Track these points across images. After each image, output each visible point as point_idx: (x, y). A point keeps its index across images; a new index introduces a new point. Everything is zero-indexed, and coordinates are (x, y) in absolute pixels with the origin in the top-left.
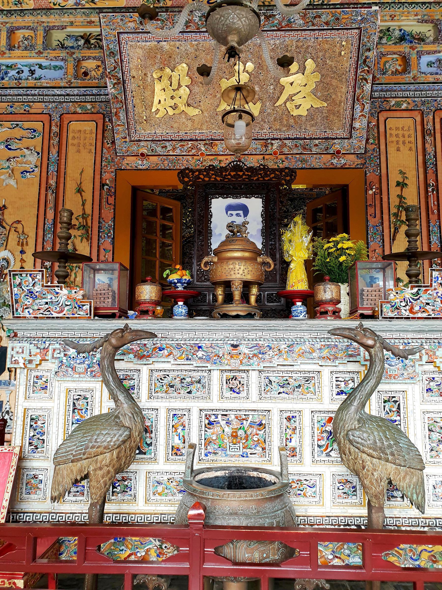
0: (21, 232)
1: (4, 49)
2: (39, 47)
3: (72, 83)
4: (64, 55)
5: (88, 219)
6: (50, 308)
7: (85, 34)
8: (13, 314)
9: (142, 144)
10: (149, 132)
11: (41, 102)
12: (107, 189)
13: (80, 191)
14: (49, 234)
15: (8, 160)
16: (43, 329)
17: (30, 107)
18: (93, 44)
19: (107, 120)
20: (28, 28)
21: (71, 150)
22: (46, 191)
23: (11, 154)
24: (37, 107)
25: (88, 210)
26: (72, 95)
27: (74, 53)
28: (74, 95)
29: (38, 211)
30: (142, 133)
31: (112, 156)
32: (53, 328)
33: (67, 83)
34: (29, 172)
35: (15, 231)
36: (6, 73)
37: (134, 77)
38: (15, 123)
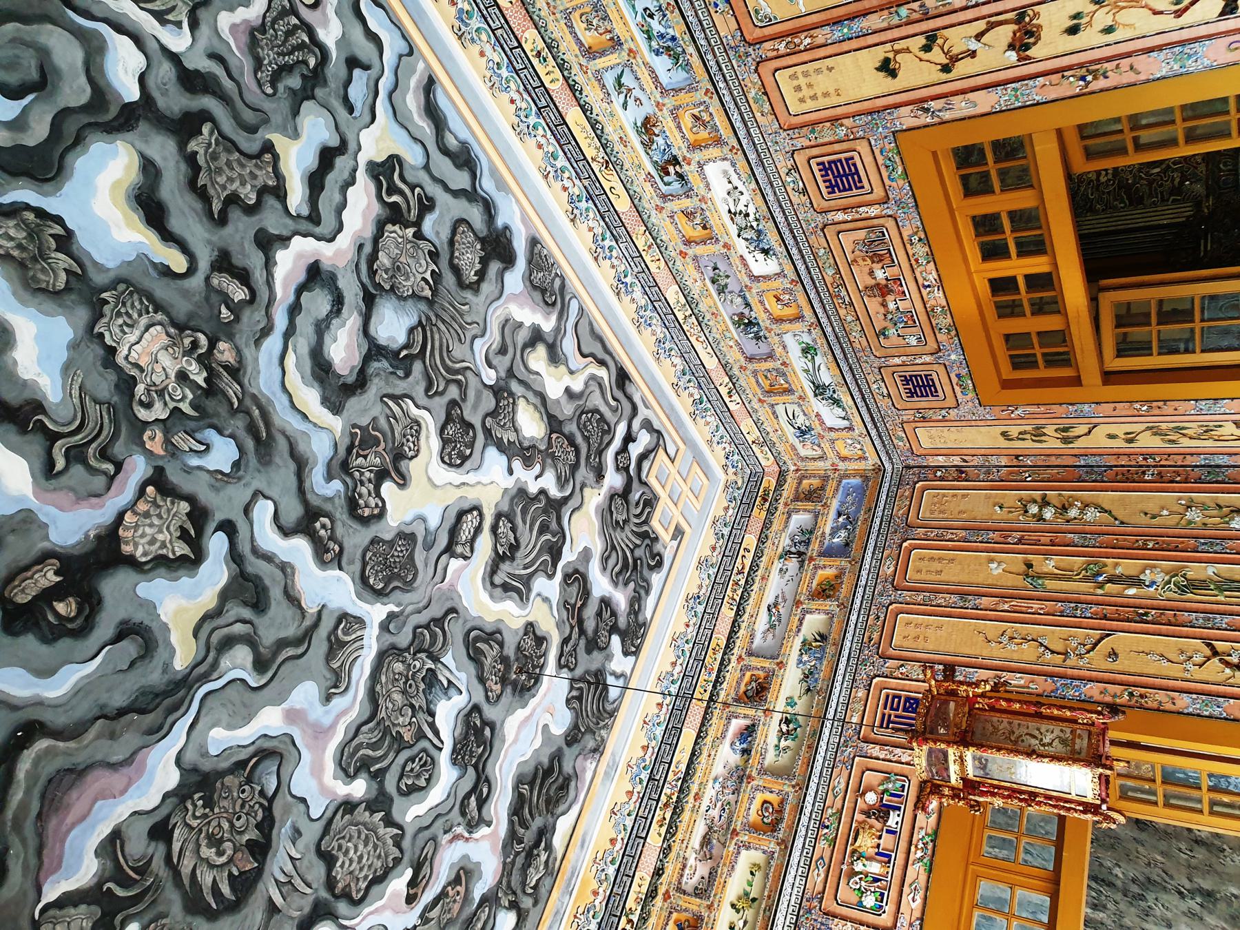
1: (625, 54)
36: (662, 36)
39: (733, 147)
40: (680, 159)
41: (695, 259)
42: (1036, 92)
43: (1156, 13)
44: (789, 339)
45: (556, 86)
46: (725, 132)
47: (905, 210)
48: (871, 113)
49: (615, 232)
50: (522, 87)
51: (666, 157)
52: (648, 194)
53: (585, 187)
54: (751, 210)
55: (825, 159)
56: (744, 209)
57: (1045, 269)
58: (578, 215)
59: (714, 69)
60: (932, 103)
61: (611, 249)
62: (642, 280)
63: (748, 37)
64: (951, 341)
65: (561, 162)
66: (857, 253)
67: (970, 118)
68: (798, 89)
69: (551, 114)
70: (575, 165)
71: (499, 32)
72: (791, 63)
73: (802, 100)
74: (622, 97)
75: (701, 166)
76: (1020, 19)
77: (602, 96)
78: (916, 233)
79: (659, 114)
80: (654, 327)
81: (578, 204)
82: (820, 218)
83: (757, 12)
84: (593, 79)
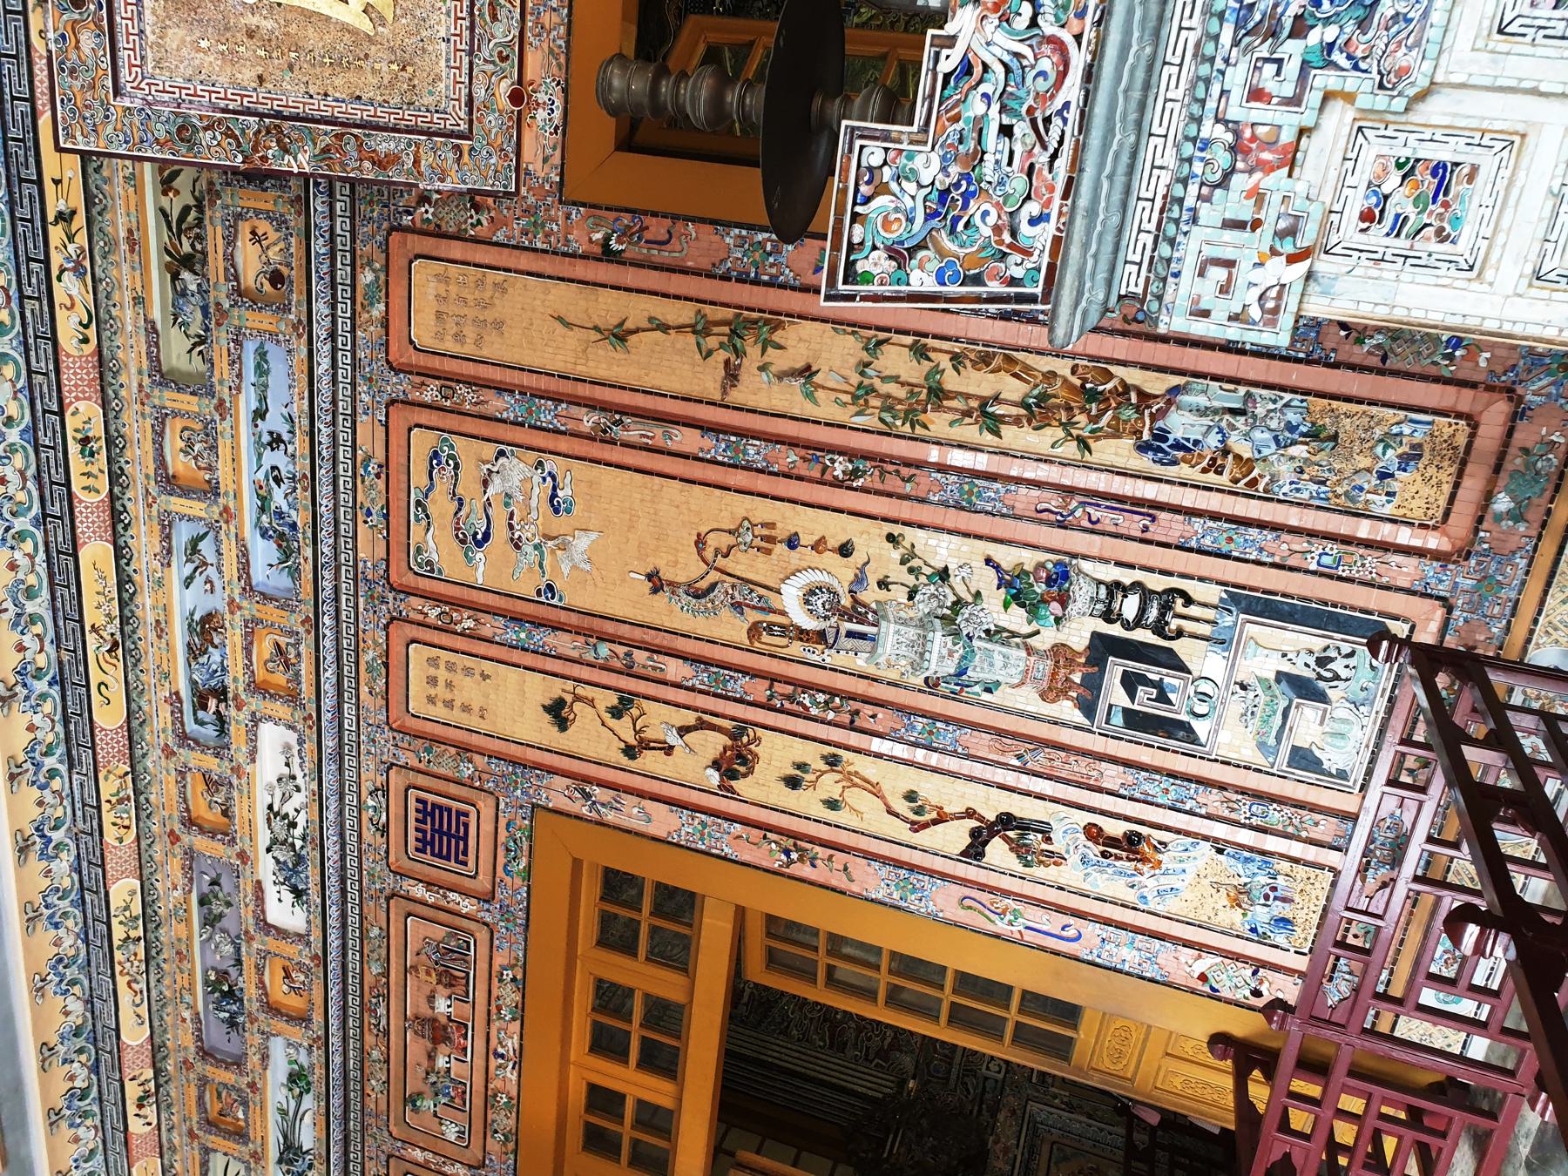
0: (731, 540)
1: (216, 510)
2: (207, 406)
3: (300, 321)
4: (224, 334)
5: (710, 318)
6: (1030, 110)
7: (168, 266)
8: (1032, 299)
9: (480, 93)
10: (443, 63)
11: (354, 423)
12: (619, 241)
13: (620, 335)
14: (745, 453)
15: (518, 547)
16: (1134, 155)
17: (368, 459)
18: (193, 246)
19: (406, 220)
20: (159, 435)
21: (493, 349)
22: (613, 442)
23: (500, 533)
24: (369, 437)
25: (682, 313)
26: (334, 323)
27: (218, 304)
28: (334, 316)
29: (674, 478)
30: (447, 87)
31: (518, 213)
32: (1136, 94)
33: (300, 336)
34: (554, 488)
35: (726, 556)
36: (280, 514)
37: (261, 79)
38: (412, 509)
39: (310, 716)
40: (230, 695)
41: (190, 854)
42: (729, 841)
43: (890, 812)
44: (277, 1048)
45: (90, 494)
46: (307, 690)
47: (510, 925)
48: (514, 763)
49: (74, 752)
50: (32, 471)
51: (213, 683)
52: (160, 720)
53: (60, 663)
54: (301, 820)
55: (431, 798)
56: (292, 813)
57: (666, 1102)
58: (21, 697)
59: (327, 592)
60: (597, 790)
61: (53, 773)
62: (82, 846)
63: (394, 578)
64: (504, 1157)
65: (38, 606)
66: (423, 957)
67: (638, 834)
68: (433, 681)
69: (60, 532)
70: (61, 623)
71: (38, 379)
72: (436, 641)
73: (431, 700)
74: (189, 568)
75: (255, 720)
76: (735, 736)
77: (158, 550)
78: (512, 967)
79: (228, 616)
80: (62, 932)
81: (29, 680)
82: (391, 879)
83: (419, 551)
84: (155, 521)
